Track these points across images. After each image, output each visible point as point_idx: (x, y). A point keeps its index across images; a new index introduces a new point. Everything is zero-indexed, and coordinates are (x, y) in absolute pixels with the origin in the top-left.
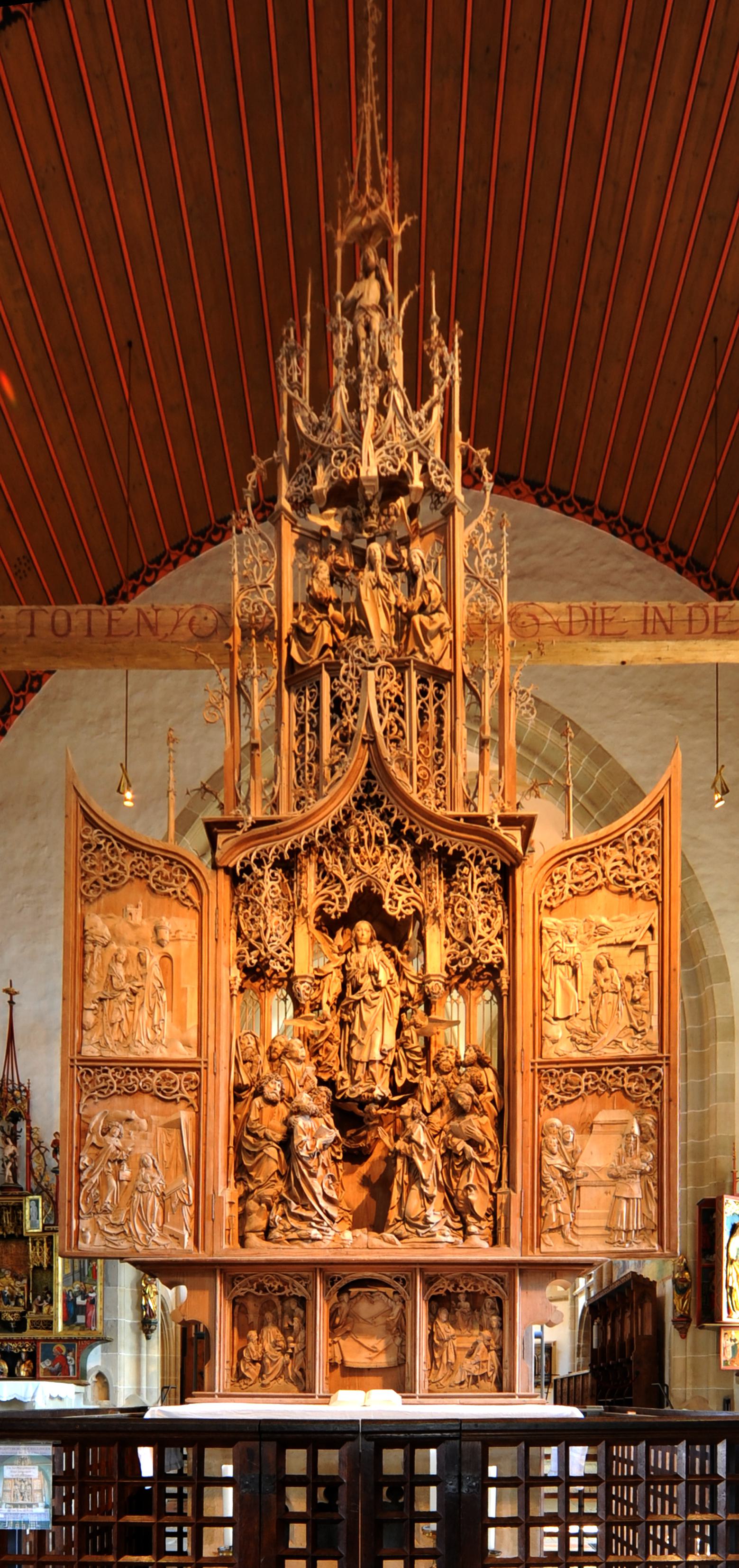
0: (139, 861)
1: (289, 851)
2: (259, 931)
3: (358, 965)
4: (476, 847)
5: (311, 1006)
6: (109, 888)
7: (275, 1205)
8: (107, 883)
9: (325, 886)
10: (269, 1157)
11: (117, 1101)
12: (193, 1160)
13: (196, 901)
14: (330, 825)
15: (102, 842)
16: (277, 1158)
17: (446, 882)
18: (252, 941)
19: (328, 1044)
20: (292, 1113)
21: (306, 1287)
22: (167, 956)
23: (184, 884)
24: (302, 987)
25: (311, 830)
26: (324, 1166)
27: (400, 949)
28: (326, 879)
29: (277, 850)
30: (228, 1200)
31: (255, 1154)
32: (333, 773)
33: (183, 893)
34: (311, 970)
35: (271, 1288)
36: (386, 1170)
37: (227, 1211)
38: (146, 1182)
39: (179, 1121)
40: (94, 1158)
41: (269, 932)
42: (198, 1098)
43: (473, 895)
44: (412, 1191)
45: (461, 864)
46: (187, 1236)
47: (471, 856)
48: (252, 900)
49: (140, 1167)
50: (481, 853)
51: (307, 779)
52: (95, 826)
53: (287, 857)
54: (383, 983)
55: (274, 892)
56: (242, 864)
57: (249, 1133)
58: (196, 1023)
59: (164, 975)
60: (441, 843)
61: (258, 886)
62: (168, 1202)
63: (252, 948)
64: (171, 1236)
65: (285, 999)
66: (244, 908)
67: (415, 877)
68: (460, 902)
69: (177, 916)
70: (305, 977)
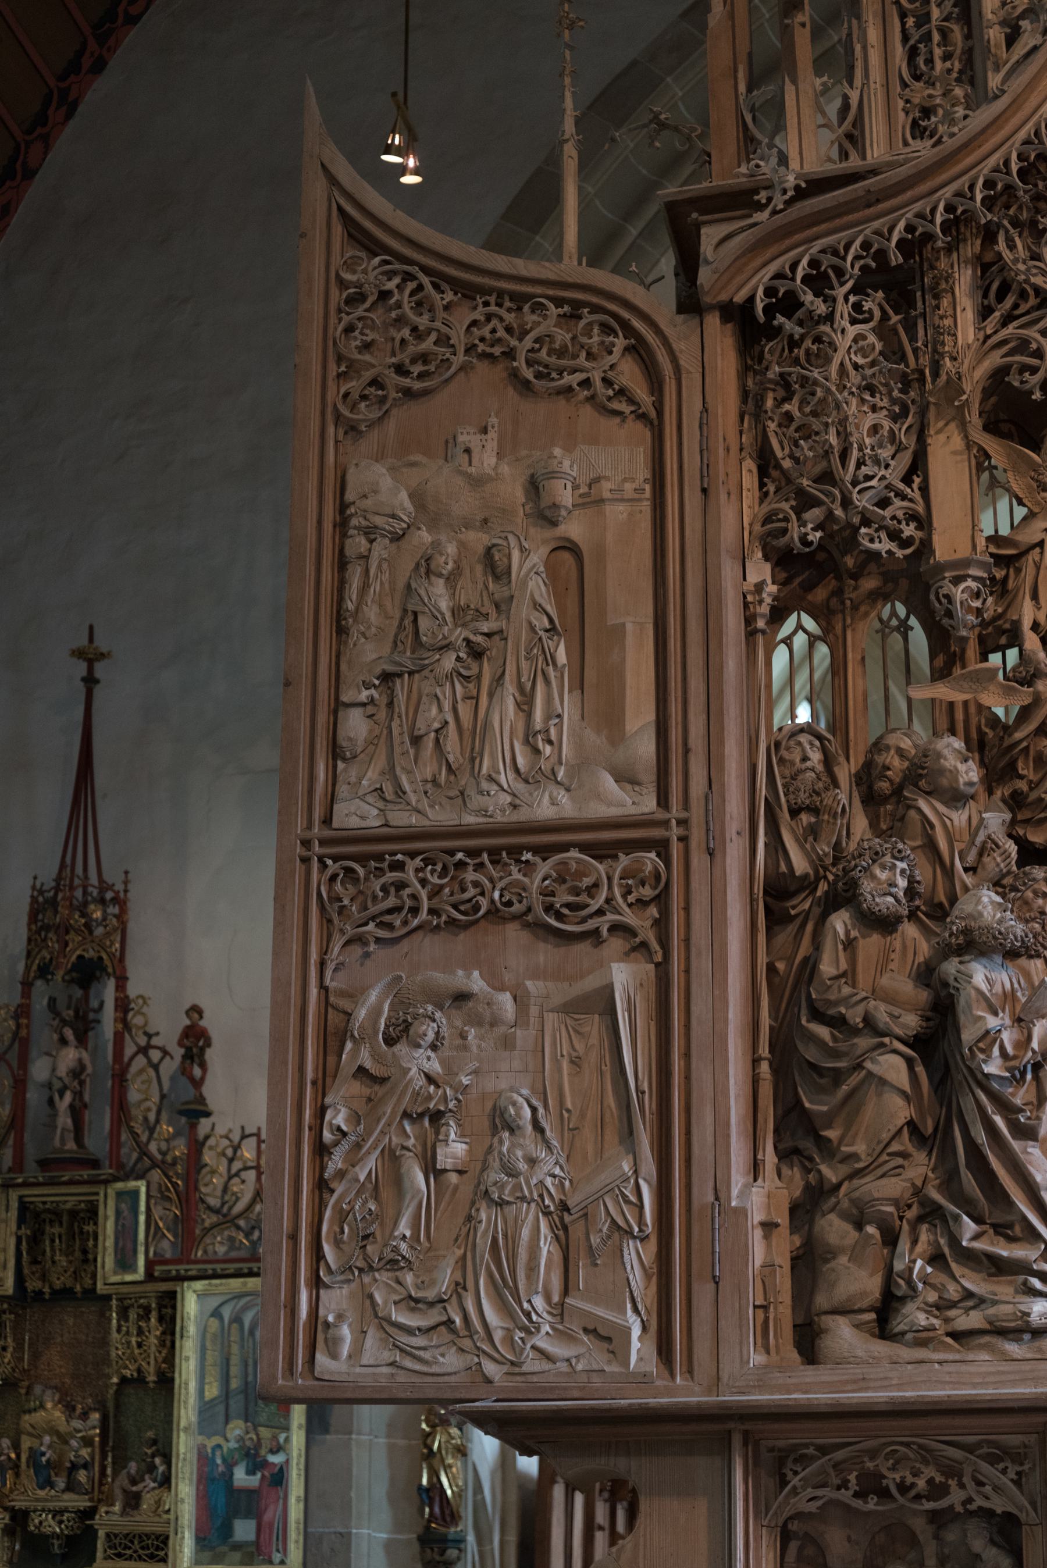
0: (489, 318)
6: (408, 393)
7: (906, 1227)
8: (406, 382)
10: (882, 1082)
11: (429, 946)
12: (650, 1103)
13: (642, 394)
14: (1014, 168)
15: (391, 285)
18: (805, 482)
20: (948, 951)
21: (1017, 1483)
22: (570, 547)
23: (613, 359)
24: (959, 593)
25: (964, 182)
29: (866, 246)
30: (758, 1216)
31: (837, 1077)
32: (1011, 41)
33: (607, 382)
34: (981, 543)
35: (904, 1488)
37: (758, 1253)
38: (512, 1173)
39: (607, 993)
40: (362, 1108)
41: (855, 454)
42: (662, 924)
46: (636, 1332)
48: (804, 381)
49: (495, 1131)
51: (939, 65)
52: (372, 247)
53: (895, 258)
55: (863, 352)
56: (770, 292)
57: (817, 1015)
58: (650, 716)
59: (559, 595)
61: (817, 340)
62: (577, 1231)
63: (805, 502)
64: (586, 1330)
66: (779, 403)
69: (593, 440)
70: (966, 563)
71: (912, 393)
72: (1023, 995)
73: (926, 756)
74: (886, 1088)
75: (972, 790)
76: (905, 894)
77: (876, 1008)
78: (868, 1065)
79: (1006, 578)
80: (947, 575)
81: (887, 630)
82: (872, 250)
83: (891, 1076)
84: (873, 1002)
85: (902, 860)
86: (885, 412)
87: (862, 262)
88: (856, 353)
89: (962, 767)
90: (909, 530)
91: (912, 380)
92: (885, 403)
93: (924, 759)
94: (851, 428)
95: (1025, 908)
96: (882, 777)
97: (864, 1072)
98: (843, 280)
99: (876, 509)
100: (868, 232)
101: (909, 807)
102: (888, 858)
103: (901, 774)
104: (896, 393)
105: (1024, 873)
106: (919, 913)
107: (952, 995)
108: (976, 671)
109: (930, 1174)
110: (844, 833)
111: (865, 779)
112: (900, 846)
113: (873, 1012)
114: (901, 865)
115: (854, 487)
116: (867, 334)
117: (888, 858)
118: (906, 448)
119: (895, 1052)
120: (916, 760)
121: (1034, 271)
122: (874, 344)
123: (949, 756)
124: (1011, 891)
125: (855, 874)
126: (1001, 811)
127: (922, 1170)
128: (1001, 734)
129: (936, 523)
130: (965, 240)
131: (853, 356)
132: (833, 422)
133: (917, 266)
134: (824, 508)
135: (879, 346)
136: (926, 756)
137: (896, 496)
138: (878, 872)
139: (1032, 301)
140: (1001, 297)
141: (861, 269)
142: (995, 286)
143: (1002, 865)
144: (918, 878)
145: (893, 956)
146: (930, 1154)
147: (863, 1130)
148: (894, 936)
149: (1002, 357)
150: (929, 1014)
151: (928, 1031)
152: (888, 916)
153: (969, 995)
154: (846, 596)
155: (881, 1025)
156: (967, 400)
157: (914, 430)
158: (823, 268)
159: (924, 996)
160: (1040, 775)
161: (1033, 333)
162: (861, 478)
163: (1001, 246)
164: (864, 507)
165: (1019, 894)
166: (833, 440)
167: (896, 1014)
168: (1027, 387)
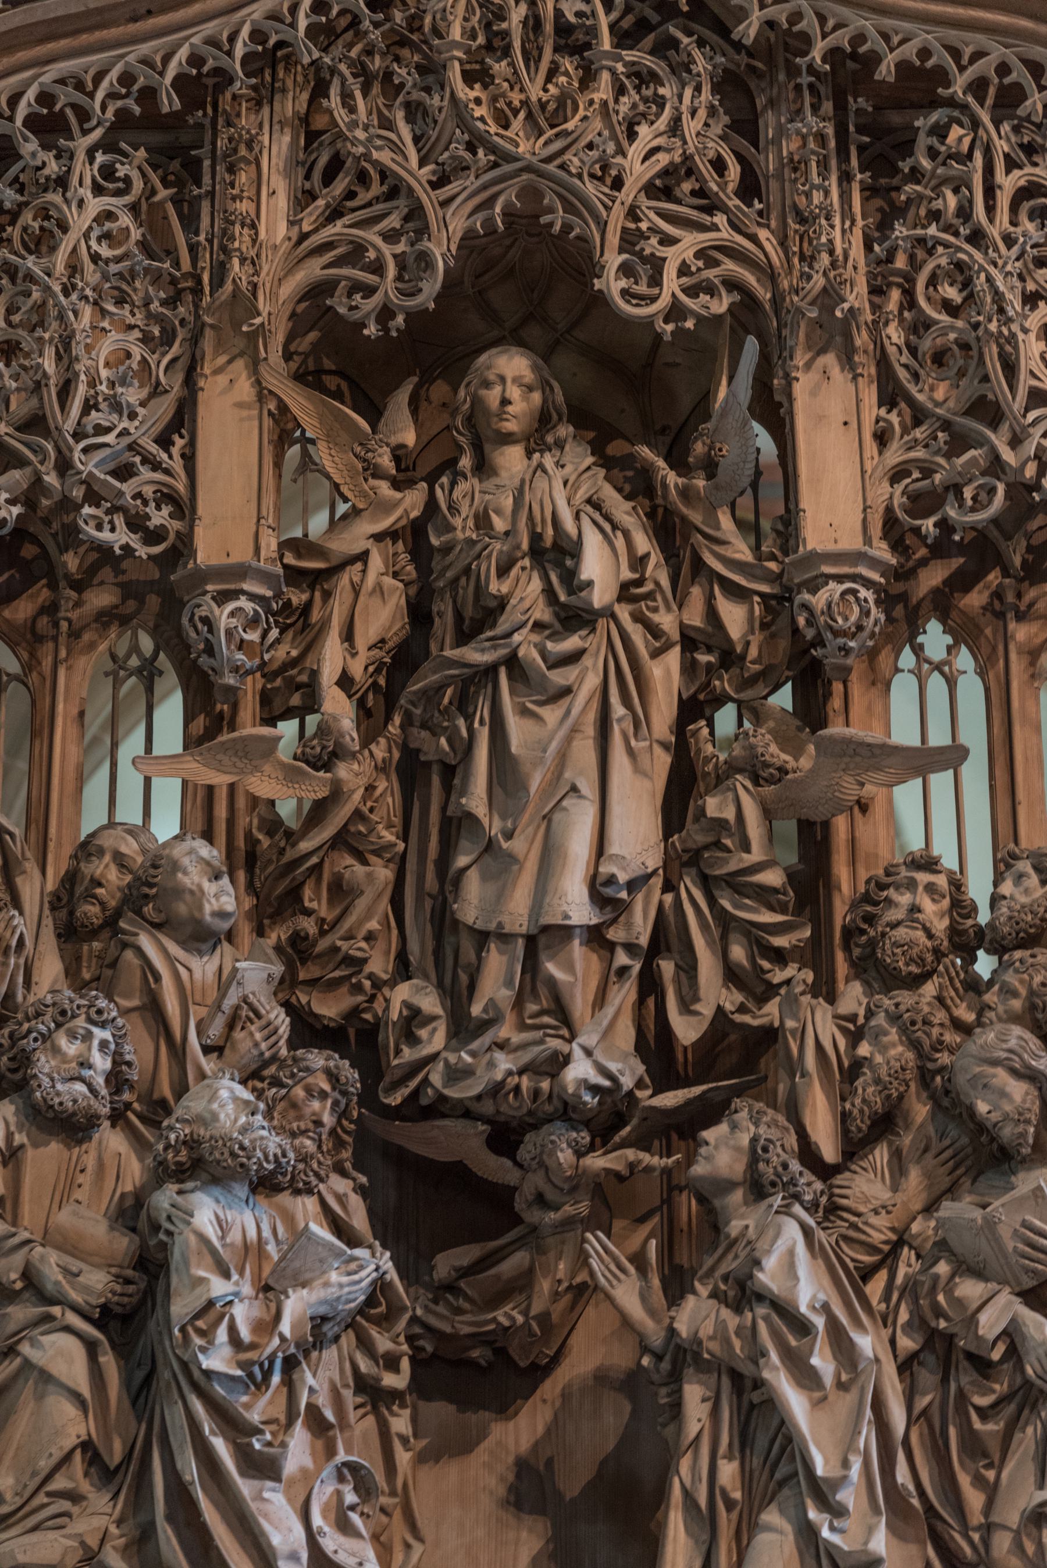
1: (180, 81)
2: (38, 387)
3: (482, 521)
4: (997, 52)
5: (265, 698)
9: (334, 214)
10: (46, 1377)
16: (81, 1381)
17: (870, 191)
19: (346, 863)
26: (317, 1424)
27: (678, 462)
28: (340, 186)
29: (127, 79)
36: (627, 1440)
41: (82, 390)
43: (994, 232)
44: (763, 1539)
45: (936, 116)
47: (979, 87)
50: (1019, 74)
53: (169, 102)
54: (600, 596)
60: (842, 39)
65: (149, 674)
67: (734, 171)
68: (942, 259)
70: (241, 572)
71: (181, 309)
72: (279, 1251)
73: (155, 866)
74: (51, 1388)
75: (226, 925)
76: (107, 1081)
77: (42, 1258)
78: (25, 1349)
79: (308, 606)
80: (209, 587)
81: (122, 673)
82: (136, 87)
83: (58, 1369)
84: (39, 1249)
85: (103, 1025)
86: (137, 334)
87: (119, 103)
88: (99, 240)
89: (210, 888)
90: (159, 517)
91: (184, 289)
92: (139, 319)
93: (152, 871)
94: (78, 350)
95: (292, 1114)
96: (90, 896)
97: (18, 1361)
98: (86, 126)
99: (109, 478)
100: (131, 58)
101: (125, 945)
102: (81, 1022)
103: (119, 895)
104: (155, 306)
105: (295, 1060)
106: (130, 1114)
107: (166, 1244)
108: (243, 739)
109: (113, 1530)
110: (20, 980)
111: (65, 900)
112: (102, 1003)
113: (37, 1264)
114: (106, 1034)
115: (77, 442)
116: (119, 212)
117: (81, 1022)
118: (166, 391)
119: (68, 1329)
120: (141, 872)
121: (379, 143)
122: (127, 229)
123: (190, 869)
124: (272, 1085)
125: (29, 1043)
126: (269, 961)
127: (100, 1522)
128: (282, 844)
129: (202, 508)
130: (284, 90)
131: (93, 243)
132: (52, 339)
133: (207, 122)
134: (28, 470)
135: (136, 234)
136: (155, 866)
137: (143, 463)
138: (63, 1041)
139: (376, 189)
140: (328, 179)
141: (118, 113)
142: (323, 160)
143: (264, 1046)
144: (128, 1057)
145: (81, 1179)
146: (115, 1496)
147: (11, 1453)
148: (84, 1147)
149: (325, 267)
150: (129, 1273)
151: (126, 1300)
152: (74, 1114)
153: (186, 1242)
154: (62, 614)
155: (49, 1287)
156: (263, 324)
157: (181, 365)
158: (58, 107)
159: (123, 1244)
160: (337, 911)
161: (371, 236)
162: (90, 429)
163: (334, 100)
164: (90, 473)
165: (284, 1091)
166: (49, 364)
167: (74, 1269)
168: (357, 315)
